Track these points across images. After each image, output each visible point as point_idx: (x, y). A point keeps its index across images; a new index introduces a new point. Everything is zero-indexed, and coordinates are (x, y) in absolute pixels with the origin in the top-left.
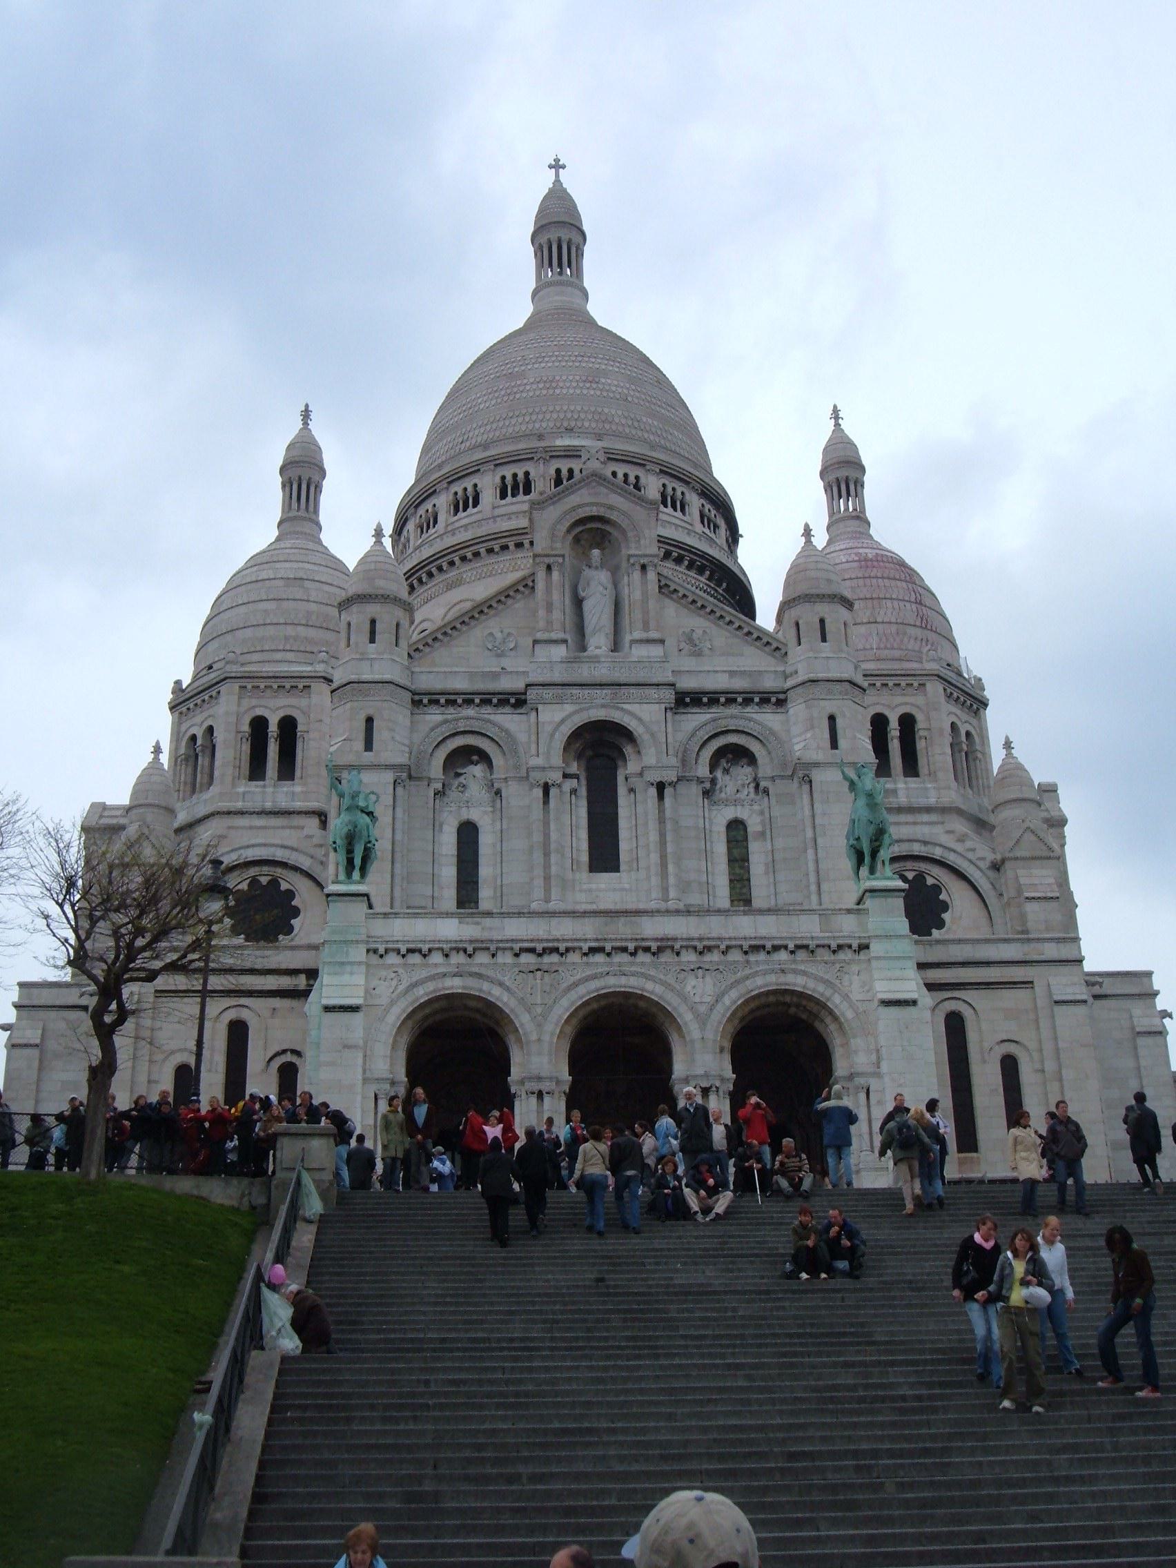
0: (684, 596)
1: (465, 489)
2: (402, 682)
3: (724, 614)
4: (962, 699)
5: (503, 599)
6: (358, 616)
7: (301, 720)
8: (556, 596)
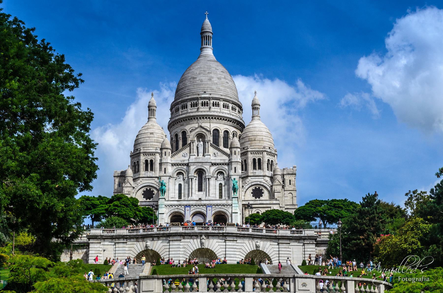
7: (154, 160)
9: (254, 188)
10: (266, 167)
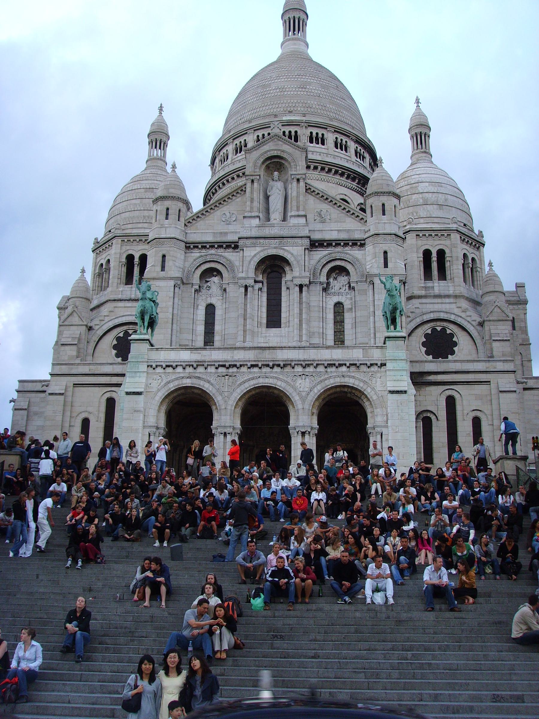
0: (318, 194)
1: (241, 142)
2: (180, 238)
3: (337, 202)
4: (470, 242)
5: (231, 197)
6: (161, 207)
8: (255, 195)
9: (429, 331)
10: (461, 272)
